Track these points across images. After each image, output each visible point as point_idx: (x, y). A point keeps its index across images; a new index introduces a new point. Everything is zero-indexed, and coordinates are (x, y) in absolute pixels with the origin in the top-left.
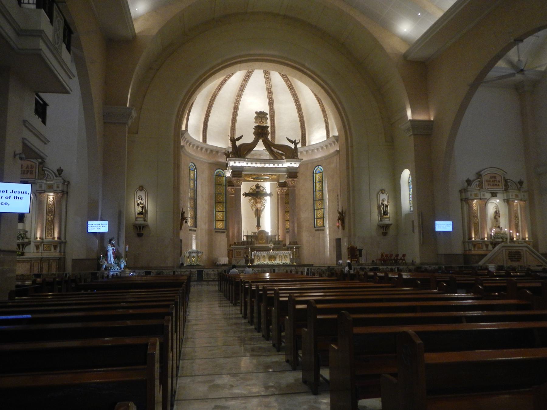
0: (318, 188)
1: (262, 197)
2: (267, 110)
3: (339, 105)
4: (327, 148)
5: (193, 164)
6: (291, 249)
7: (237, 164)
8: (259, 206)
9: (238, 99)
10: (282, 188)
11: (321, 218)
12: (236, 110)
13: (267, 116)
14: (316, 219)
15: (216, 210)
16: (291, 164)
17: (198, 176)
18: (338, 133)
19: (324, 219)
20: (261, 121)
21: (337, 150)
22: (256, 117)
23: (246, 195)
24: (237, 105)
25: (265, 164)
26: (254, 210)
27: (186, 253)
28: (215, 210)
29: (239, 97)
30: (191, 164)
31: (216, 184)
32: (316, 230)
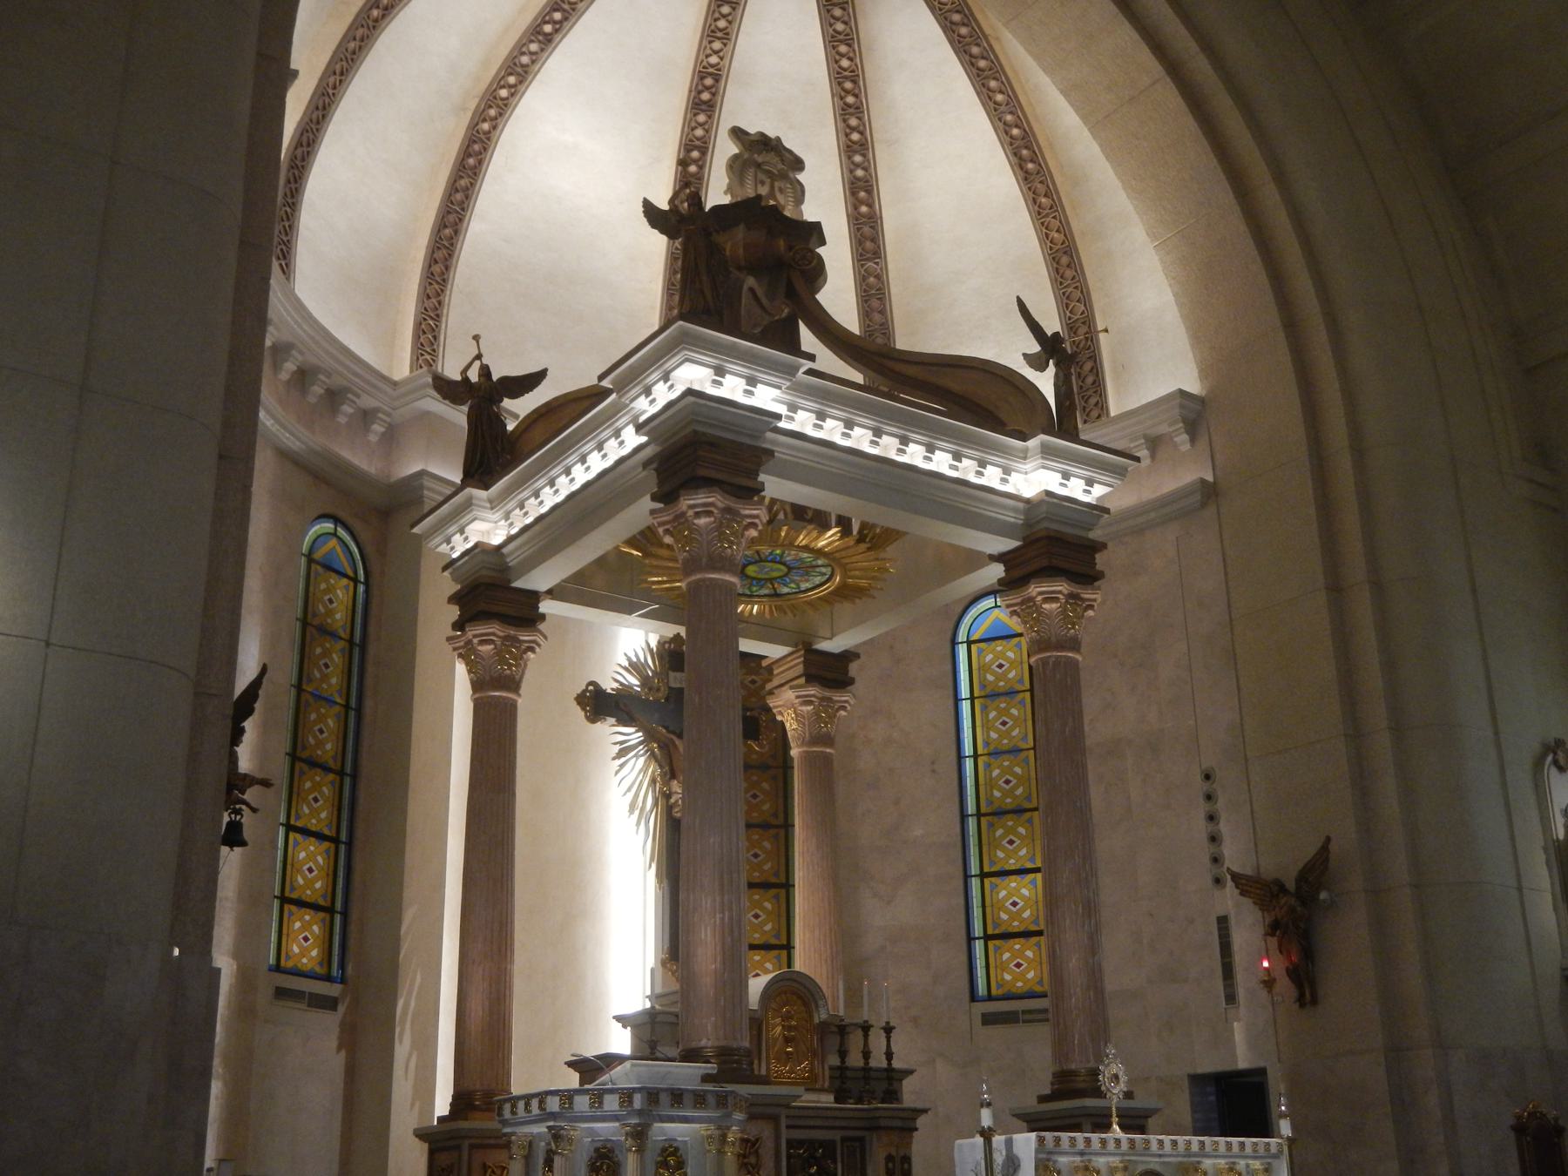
3: (1269, 196)
7: (732, 388)
9: (504, 93)
10: (827, 694)
11: (1026, 934)
12: (471, 161)
13: (801, 177)
14: (987, 938)
15: (292, 822)
16: (1066, 476)
21: (1203, 481)
22: (735, 157)
25: (905, 441)
27: (582, 1103)
28: (282, 819)
29: (512, 80)
31: (305, 623)
32: (988, 1019)
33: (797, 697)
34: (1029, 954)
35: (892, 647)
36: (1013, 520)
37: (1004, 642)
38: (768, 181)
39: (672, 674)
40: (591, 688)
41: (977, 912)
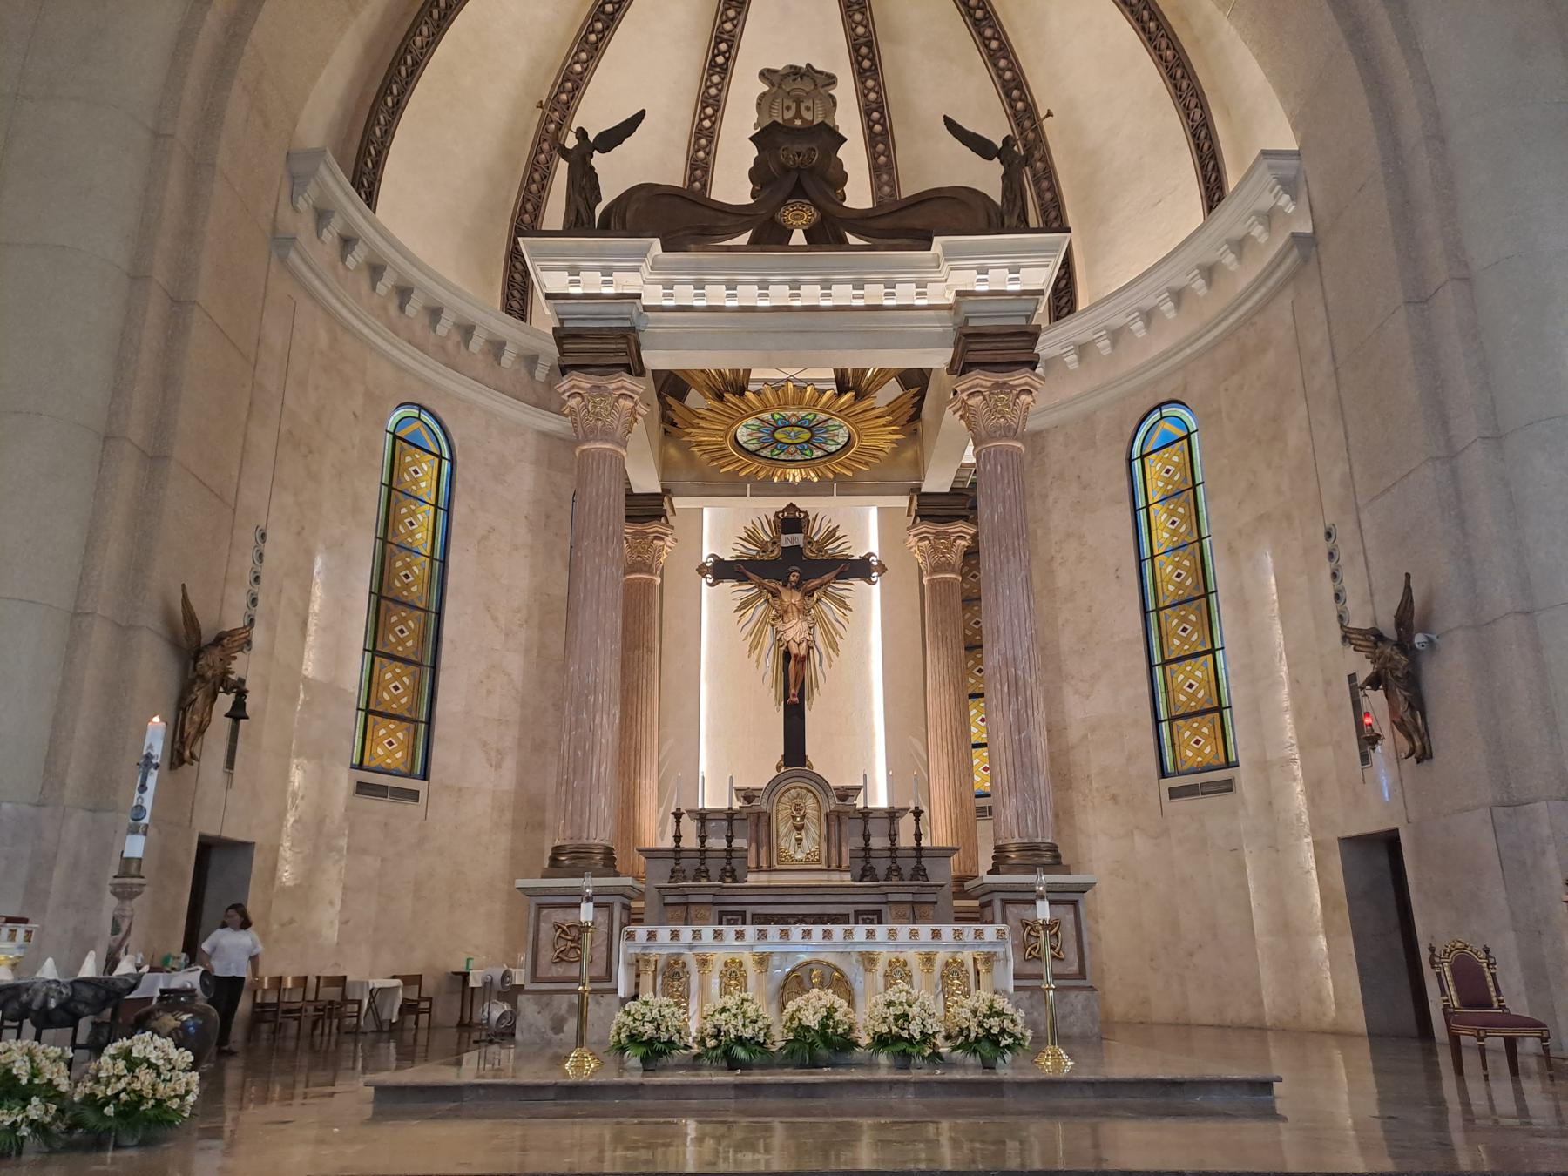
0: (1163, 537)
1: (817, 582)
2: (835, 59)
4: (1210, 282)
5: (425, 417)
6: (1012, 909)
7: (591, 282)
8: (795, 630)
9: (707, 123)
10: (941, 528)
14: (1171, 720)
16: (983, 270)
17: (458, 486)
18: (1295, 127)
19: (1227, 713)
20: (798, 115)
22: (763, 96)
23: (722, 570)
24: (701, 154)
26: (769, 662)
30: (415, 412)
32: (1175, 793)
33: (915, 536)
34: (1205, 730)
35: (1079, 477)
36: (941, 329)
37: (1170, 448)
38: (794, 106)
39: (783, 537)
40: (711, 559)
41: (1161, 698)
